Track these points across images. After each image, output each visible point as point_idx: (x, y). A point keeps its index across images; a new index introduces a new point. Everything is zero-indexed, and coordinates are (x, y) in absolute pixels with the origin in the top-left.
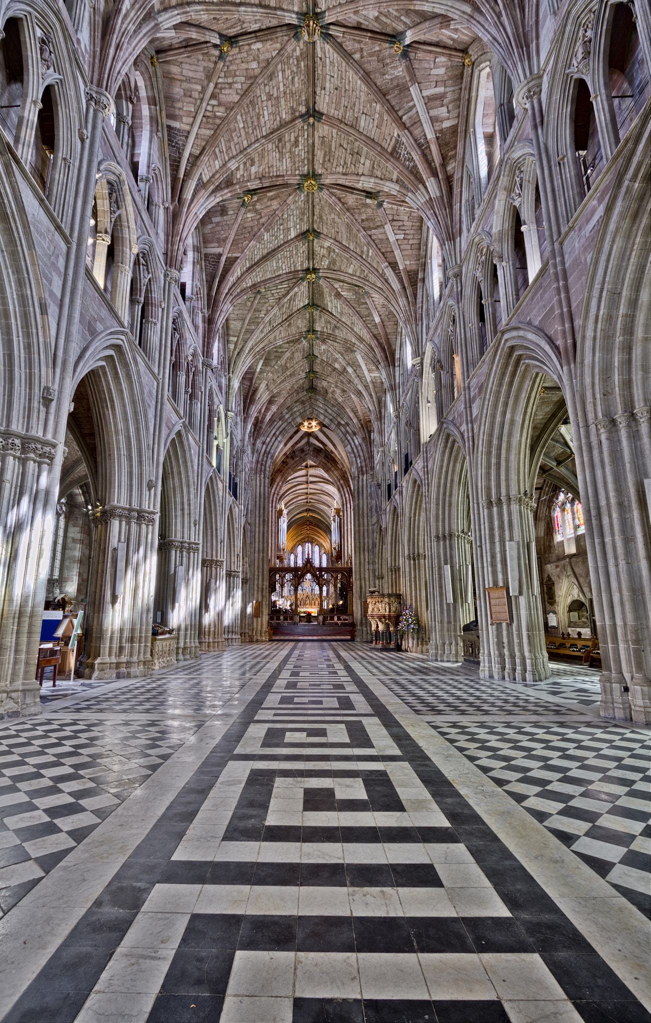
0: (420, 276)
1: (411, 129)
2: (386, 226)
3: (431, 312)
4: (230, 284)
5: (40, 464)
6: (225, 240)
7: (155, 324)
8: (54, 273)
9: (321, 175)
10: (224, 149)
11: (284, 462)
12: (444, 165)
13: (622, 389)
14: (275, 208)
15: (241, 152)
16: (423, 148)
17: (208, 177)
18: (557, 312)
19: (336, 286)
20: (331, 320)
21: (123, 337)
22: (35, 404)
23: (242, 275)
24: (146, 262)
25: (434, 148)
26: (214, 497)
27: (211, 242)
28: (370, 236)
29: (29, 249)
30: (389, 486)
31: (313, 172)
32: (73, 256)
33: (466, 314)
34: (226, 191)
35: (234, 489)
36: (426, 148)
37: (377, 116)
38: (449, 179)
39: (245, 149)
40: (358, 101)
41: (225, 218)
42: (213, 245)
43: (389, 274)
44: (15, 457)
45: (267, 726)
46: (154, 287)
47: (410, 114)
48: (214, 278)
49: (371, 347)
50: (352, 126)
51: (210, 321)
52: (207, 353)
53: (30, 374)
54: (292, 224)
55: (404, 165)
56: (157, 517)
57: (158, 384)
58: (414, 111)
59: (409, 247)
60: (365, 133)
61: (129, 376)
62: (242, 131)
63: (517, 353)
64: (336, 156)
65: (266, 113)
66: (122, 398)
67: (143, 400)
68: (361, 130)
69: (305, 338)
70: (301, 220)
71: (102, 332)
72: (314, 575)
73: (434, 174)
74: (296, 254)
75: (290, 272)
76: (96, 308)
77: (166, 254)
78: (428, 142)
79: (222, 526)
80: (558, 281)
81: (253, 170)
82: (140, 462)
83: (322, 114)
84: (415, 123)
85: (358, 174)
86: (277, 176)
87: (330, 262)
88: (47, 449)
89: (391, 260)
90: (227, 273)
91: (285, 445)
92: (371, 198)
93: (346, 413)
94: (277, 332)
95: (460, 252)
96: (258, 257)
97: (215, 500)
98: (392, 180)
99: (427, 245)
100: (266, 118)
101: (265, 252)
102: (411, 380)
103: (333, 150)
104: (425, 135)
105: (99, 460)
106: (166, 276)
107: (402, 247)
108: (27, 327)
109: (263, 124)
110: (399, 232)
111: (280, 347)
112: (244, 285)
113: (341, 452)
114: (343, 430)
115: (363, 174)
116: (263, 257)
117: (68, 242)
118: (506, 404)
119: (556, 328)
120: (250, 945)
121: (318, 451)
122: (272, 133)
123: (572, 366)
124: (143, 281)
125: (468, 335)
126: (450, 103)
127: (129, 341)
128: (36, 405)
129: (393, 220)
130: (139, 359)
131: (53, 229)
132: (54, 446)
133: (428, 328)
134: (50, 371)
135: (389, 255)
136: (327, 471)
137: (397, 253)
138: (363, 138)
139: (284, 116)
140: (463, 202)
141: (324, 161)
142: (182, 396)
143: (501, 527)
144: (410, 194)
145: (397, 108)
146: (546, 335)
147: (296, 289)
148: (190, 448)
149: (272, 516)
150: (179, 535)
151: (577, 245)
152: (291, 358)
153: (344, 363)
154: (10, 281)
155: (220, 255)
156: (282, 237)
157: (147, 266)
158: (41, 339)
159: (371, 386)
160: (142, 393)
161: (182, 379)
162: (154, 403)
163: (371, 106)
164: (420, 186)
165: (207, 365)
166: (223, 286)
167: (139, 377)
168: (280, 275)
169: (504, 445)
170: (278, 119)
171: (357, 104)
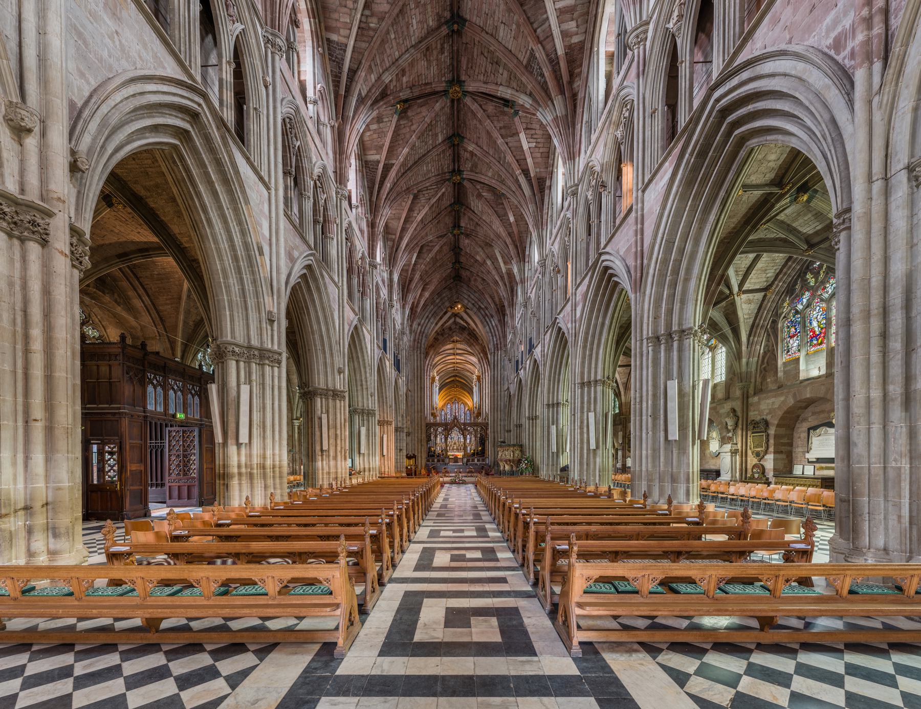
0: (548, 183)
1: (544, 43)
2: (521, 135)
3: (554, 219)
4: (387, 190)
5: (272, 367)
6: (381, 147)
7: (333, 239)
8: (263, 219)
9: (464, 82)
10: (379, 62)
11: (436, 339)
12: (571, 83)
13: (666, 315)
14: (424, 114)
15: (393, 63)
16: (554, 62)
17: (366, 92)
18: (634, 250)
19: (478, 187)
20: (474, 219)
21: (312, 258)
22: (264, 325)
23: (397, 180)
24: (321, 184)
25: (563, 65)
26: (383, 373)
27: (370, 149)
28: (507, 143)
29: (246, 204)
30: (517, 361)
31: (458, 77)
32: (273, 201)
33: (578, 229)
34: (381, 103)
35: (397, 365)
36: (556, 64)
37: (514, 26)
38: (574, 96)
39: (397, 60)
40: (497, 8)
41: (381, 124)
42: (372, 152)
43: (522, 180)
44: (256, 363)
45: (430, 528)
46: (329, 206)
47: (543, 27)
48: (374, 184)
49: (506, 243)
50: (492, 35)
51: (372, 225)
52: (372, 254)
53: (258, 302)
54: (440, 130)
55: (536, 80)
56: (347, 395)
57: (339, 290)
58: (547, 25)
59: (539, 155)
60: (503, 43)
61: (318, 289)
62: (393, 41)
63: (610, 271)
64: (478, 64)
65: (414, 21)
66: (315, 306)
67: (330, 306)
68: (500, 39)
69: (451, 233)
70: (447, 125)
71: (298, 258)
72: (460, 429)
73: (562, 92)
74: (443, 157)
75: (438, 175)
76: (292, 239)
77: (335, 172)
78: (557, 58)
79: (390, 394)
80: (637, 224)
81: (405, 79)
82: (332, 355)
83: (466, 20)
84: (547, 37)
85: (497, 84)
86: (426, 84)
87: (472, 165)
88: (276, 357)
89: (524, 167)
90: (385, 179)
91: (436, 324)
92: (508, 106)
93: (485, 298)
94: (428, 229)
95: (578, 171)
96: (411, 163)
97: (384, 375)
98: (526, 93)
99: (554, 154)
100: (415, 27)
101: (417, 157)
102: (536, 277)
103: (475, 57)
104: (556, 50)
105: (300, 352)
106: (337, 193)
107: (533, 155)
108: (252, 267)
109: (412, 33)
110: (531, 140)
111: (431, 241)
112: (398, 189)
113: (481, 329)
114: (483, 313)
115: (501, 84)
116: (415, 163)
117: (268, 188)
118: (599, 310)
119: (631, 262)
120: (427, 597)
121: (463, 329)
122: (420, 42)
123: (638, 294)
124: (320, 203)
125: (579, 248)
126: (579, 17)
127: (316, 260)
128: (264, 325)
129: (527, 129)
130: (324, 273)
131: (257, 180)
132: (280, 354)
133: (551, 234)
134: (270, 298)
135: (522, 162)
136: (470, 346)
137: (529, 160)
138: (502, 49)
139: (431, 23)
140: (584, 123)
141: (467, 68)
142: (357, 295)
143: (589, 402)
144: (540, 109)
145: (532, 20)
146: (627, 265)
147: (444, 190)
148: (364, 338)
149: (427, 383)
150: (360, 404)
151: (653, 197)
152: (440, 251)
153: (484, 256)
154: (236, 232)
155: (378, 162)
156: (431, 142)
157: (322, 188)
158: (262, 275)
159: (506, 277)
160: (329, 301)
161: (355, 281)
162: (337, 307)
163: (509, 15)
164: (549, 103)
165: (374, 266)
166: (382, 192)
167: (326, 289)
168: (430, 178)
169: (596, 342)
170: (425, 26)
171: (497, 12)
